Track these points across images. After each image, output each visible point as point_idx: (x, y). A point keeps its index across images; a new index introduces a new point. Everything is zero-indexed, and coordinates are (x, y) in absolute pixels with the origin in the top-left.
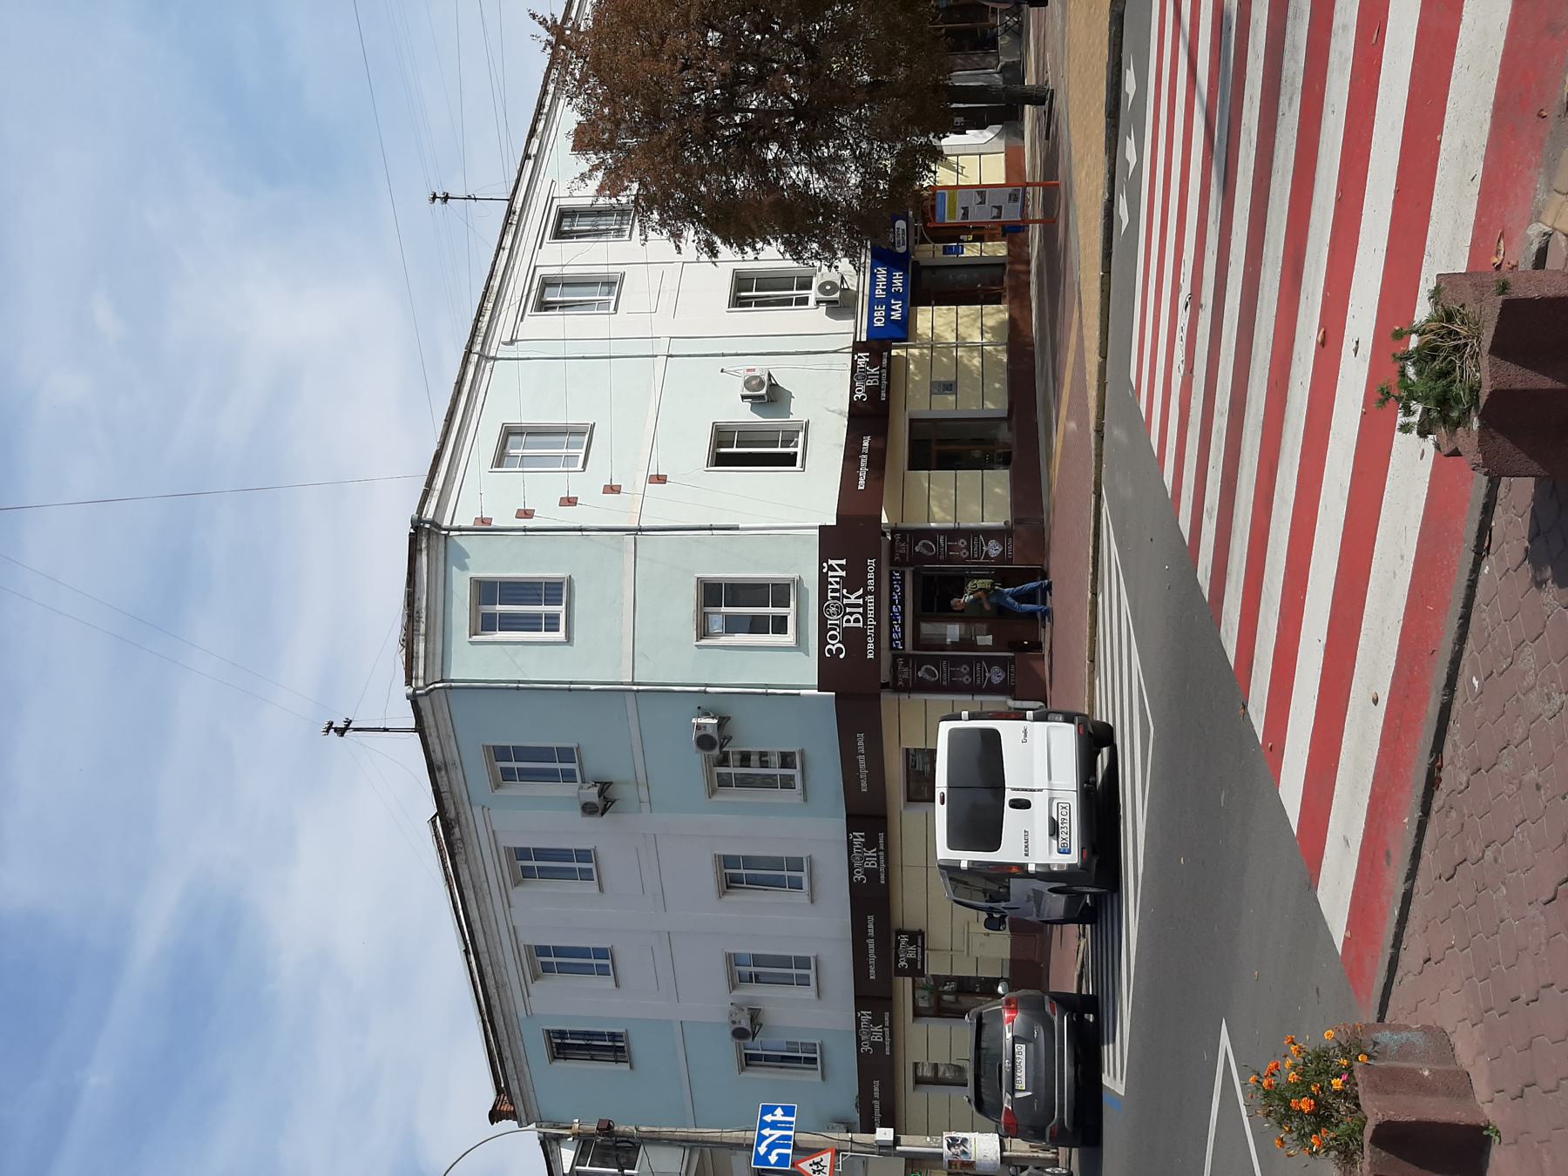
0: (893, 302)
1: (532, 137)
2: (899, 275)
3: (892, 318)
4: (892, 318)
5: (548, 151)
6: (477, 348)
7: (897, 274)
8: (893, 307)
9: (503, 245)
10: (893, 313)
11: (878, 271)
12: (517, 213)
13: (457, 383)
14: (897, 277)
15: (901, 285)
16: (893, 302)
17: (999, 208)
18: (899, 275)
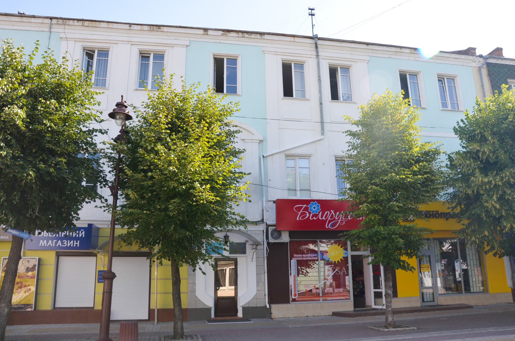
0: (54, 241)
1: (223, 31)
2: (77, 245)
3: (41, 241)
4: (41, 241)
5: (215, 41)
6: (54, 21)
7: (78, 243)
8: (50, 241)
9: (132, 25)
10: (45, 241)
11: (82, 232)
12: (159, 30)
13: (34, 16)
14: (75, 243)
15: (68, 245)
16: (54, 241)
18: (77, 245)
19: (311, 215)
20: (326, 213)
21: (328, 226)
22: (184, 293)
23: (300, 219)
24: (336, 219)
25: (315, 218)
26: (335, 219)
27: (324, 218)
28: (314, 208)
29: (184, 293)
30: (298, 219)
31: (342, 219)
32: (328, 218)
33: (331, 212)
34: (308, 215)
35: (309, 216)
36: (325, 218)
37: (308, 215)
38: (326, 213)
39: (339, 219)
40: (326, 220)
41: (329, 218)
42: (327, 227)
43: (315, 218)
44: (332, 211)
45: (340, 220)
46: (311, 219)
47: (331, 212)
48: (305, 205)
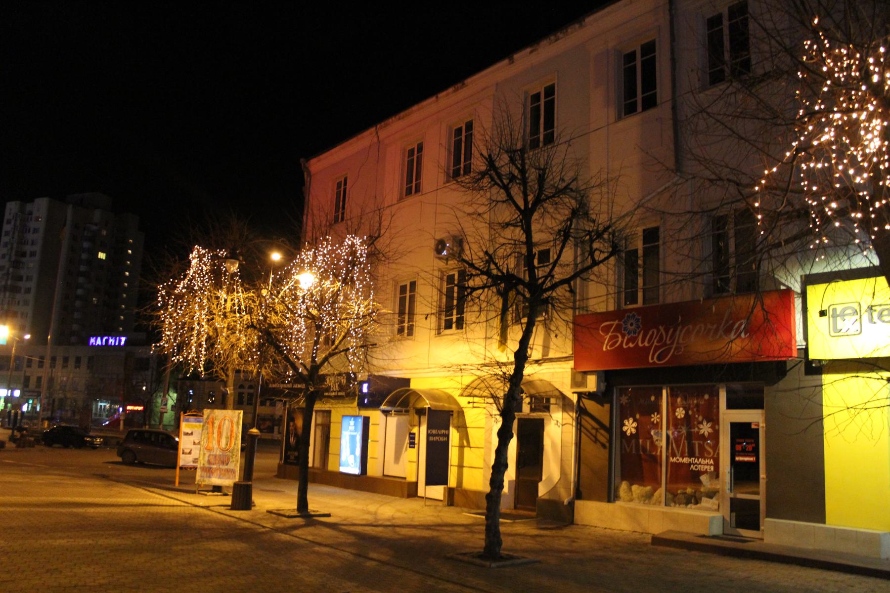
17: (190, 453)
19: (626, 338)
20: (650, 333)
21: (653, 358)
22: (454, 466)
23: (608, 347)
24: (668, 342)
25: (631, 345)
26: (665, 344)
27: (646, 344)
28: (632, 325)
29: (454, 466)
30: (604, 349)
31: (678, 343)
32: (653, 343)
33: (658, 331)
34: (620, 339)
35: (622, 342)
36: (648, 343)
37: (620, 339)
38: (650, 333)
39: (672, 343)
40: (649, 348)
41: (655, 343)
42: (651, 361)
43: (631, 345)
44: (660, 327)
45: (674, 346)
46: (625, 347)
47: (660, 330)
48: (617, 322)
